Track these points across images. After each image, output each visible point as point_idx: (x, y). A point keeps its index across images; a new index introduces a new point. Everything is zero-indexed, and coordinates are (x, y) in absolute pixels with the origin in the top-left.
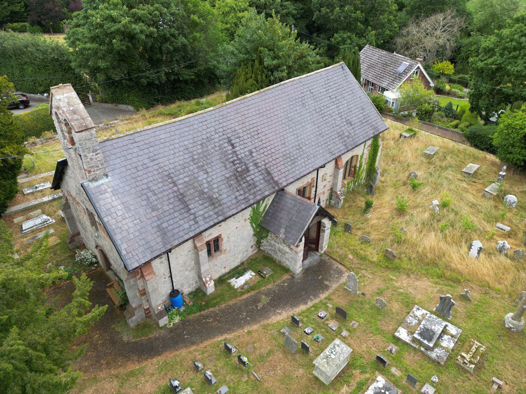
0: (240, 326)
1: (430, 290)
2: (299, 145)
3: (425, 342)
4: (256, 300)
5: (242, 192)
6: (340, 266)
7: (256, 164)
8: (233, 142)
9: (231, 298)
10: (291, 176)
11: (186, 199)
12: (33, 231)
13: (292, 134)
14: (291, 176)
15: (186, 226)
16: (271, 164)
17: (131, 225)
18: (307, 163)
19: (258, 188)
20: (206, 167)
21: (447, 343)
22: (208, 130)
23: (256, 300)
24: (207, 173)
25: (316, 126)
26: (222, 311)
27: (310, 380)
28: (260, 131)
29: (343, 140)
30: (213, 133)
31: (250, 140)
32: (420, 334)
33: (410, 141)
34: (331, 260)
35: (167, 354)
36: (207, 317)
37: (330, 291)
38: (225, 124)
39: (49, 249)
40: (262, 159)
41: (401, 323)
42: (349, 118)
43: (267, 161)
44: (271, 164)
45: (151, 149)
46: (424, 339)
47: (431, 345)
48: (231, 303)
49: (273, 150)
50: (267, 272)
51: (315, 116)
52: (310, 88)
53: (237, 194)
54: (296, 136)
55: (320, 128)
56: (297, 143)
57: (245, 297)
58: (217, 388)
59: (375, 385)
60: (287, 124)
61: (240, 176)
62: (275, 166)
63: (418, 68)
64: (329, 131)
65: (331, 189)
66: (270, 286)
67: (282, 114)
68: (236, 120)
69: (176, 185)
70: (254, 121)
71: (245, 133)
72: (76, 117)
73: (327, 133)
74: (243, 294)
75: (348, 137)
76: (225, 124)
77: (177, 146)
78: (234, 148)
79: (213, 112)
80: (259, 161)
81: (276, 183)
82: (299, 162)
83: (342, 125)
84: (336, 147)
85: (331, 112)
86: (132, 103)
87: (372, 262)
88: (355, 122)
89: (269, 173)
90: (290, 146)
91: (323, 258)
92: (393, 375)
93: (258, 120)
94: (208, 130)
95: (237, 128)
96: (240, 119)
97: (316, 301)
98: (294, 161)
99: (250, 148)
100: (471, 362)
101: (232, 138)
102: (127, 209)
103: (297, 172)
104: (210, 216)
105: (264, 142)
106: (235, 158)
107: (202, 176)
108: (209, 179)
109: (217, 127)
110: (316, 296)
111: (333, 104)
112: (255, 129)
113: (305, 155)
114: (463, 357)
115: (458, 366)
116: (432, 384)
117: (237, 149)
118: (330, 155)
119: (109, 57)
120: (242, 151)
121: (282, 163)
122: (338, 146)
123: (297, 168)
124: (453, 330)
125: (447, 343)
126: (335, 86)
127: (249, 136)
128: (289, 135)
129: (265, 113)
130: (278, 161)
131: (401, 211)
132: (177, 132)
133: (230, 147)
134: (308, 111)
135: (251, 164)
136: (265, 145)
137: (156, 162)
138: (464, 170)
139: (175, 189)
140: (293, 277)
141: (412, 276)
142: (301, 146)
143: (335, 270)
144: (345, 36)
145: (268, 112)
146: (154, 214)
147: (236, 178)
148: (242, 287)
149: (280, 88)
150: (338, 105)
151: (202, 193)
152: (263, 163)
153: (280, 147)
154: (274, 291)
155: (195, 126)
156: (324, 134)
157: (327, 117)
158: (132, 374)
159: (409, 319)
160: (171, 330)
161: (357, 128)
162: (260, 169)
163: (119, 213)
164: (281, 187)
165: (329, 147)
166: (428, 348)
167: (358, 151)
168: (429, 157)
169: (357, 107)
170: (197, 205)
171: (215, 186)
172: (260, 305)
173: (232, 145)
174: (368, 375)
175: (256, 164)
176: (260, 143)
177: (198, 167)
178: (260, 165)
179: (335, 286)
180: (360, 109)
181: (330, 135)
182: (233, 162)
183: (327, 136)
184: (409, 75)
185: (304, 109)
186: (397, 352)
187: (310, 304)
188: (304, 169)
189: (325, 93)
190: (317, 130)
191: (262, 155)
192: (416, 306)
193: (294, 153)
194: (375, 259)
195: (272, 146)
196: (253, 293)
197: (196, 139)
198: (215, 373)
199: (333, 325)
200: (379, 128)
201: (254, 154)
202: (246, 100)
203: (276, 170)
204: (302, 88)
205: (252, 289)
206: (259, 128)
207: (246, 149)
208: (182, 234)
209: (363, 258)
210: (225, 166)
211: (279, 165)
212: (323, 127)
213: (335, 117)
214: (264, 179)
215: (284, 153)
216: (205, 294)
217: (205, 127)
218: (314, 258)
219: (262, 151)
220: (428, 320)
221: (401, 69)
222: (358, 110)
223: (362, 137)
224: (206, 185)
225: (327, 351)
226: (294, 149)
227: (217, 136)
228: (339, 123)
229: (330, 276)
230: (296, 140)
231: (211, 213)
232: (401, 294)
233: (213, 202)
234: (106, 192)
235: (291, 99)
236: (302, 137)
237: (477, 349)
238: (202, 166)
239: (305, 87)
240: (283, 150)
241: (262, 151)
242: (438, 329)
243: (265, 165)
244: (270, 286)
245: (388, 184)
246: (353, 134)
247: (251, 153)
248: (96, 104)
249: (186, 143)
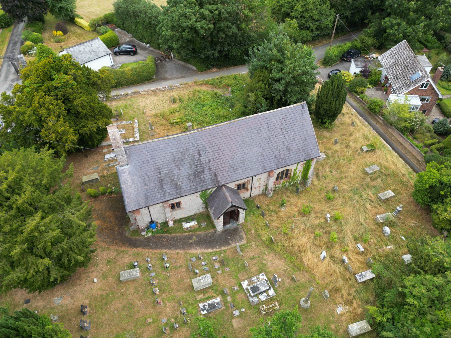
0: (176, 249)
1: (281, 267)
2: (243, 160)
3: (251, 292)
4: (190, 238)
5: (195, 184)
6: (244, 235)
8: (201, 153)
9: (179, 232)
10: (229, 179)
11: (163, 183)
12: (109, 160)
13: (242, 152)
14: (229, 179)
15: (159, 196)
16: (219, 170)
17: (133, 191)
18: (243, 173)
19: (205, 183)
20: (180, 166)
21: (263, 297)
22: (189, 144)
24: (179, 170)
25: (261, 149)
26: (172, 238)
27: (190, 286)
28: (220, 148)
29: (277, 161)
30: (191, 146)
31: (212, 153)
32: (252, 288)
33: (365, 154)
34: (242, 230)
35: (139, 249)
36: (164, 238)
37: (229, 247)
38: (199, 142)
39: (112, 174)
40: (215, 166)
41: (249, 279)
42: (290, 145)
43: (217, 168)
44: (219, 170)
45: (153, 153)
46: (251, 291)
47: (252, 295)
48: (178, 235)
49: (224, 162)
50: (203, 225)
51: (263, 141)
52: (268, 122)
53: (192, 184)
54: (244, 154)
55: (263, 151)
56: (242, 159)
57: (186, 234)
58: (151, 272)
59: (214, 300)
60: (241, 145)
61: (198, 174)
62: (222, 172)
63: (428, 81)
64: (269, 154)
65: (266, 185)
66: (201, 233)
67: (240, 139)
68: (208, 140)
69: (160, 174)
70: (220, 141)
71: (210, 149)
72: (115, 141)
73: (267, 154)
74: (186, 232)
75: (283, 159)
76: (199, 142)
77: (168, 152)
78: (200, 157)
79: (195, 134)
80: (212, 167)
81: (218, 182)
82: (238, 171)
83: (282, 150)
84: (269, 165)
85: (277, 140)
86: (195, 65)
87: (262, 240)
88: (294, 149)
89: (216, 175)
90: (237, 160)
91: (238, 227)
92: (227, 300)
93: (222, 141)
94: (189, 144)
95: (206, 145)
96: (210, 139)
97: (218, 250)
98: (235, 170)
99: (209, 158)
100: (265, 311)
101: (201, 151)
102: (133, 183)
103: (234, 178)
104: (173, 194)
105: (220, 155)
106: (199, 163)
107: (176, 171)
108: (179, 174)
109: (194, 143)
110: (220, 247)
111: (282, 134)
112: (218, 146)
113: (245, 168)
114: (263, 307)
115: (259, 309)
116: (240, 312)
117: (201, 158)
118: (263, 169)
119: (180, 42)
120: (204, 159)
121: (227, 170)
122: (272, 165)
123: (235, 175)
124: (271, 292)
125: (263, 297)
126: (289, 120)
127: (212, 150)
128: (238, 153)
129: (228, 137)
130: (225, 168)
131: (303, 214)
132: (170, 144)
133: (198, 156)
134: (260, 138)
135: (207, 168)
136: (220, 158)
137: (154, 160)
138: (379, 195)
139: (159, 176)
140: (216, 232)
141: (277, 256)
142: (244, 161)
143: (239, 236)
144: (394, 22)
145: (231, 136)
146: (145, 187)
147: (195, 176)
148: (187, 229)
149: (246, 120)
150: (285, 135)
151: (173, 180)
152: (215, 168)
153: (229, 160)
154: (201, 237)
155: (181, 142)
156: (264, 155)
157: (272, 143)
158: (123, 252)
160: (146, 239)
161: (292, 154)
162: (211, 172)
163: (129, 184)
164: (220, 184)
165: (265, 164)
166: (250, 295)
167: (293, 167)
168: (366, 174)
169: (301, 138)
170: (168, 186)
171: (181, 178)
172: (191, 241)
173: (200, 156)
174: (215, 295)
175: (210, 169)
176: (218, 156)
177: (175, 166)
178: (212, 169)
179: (233, 245)
180: (303, 139)
181: (269, 156)
182: (196, 165)
183: (266, 157)
184: (417, 85)
185: (258, 136)
186: (237, 291)
187: (215, 250)
188: (240, 176)
189: (279, 125)
190: (261, 151)
191: (216, 164)
192: (263, 273)
193: (238, 165)
194: (264, 239)
195: (224, 159)
196: (191, 233)
197: (179, 149)
198: (154, 266)
199: (217, 265)
200: (312, 155)
201: (211, 163)
202: (218, 127)
203: (221, 174)
204: (262, 121)
205: (191, 231)
206: (220, 146)
207: (207, 159)
208: (155, 200)
209: (259, 235)
210: (191, 167)
211: (224, 171)
212: (266, 150)
213: (279, 144)
214: (211, 178)
215: (231, 164)
216: (168, 225)
217: (187, 143)
218: (231, 226)
219: (217, 161)
220: (261, 283)
221: (415, 77)
222: (300, 140)
223: (293, 161)
224: (176, 177)
225: (201, 278)
226: (239, 162)
227: (193, 148)
228: (280, 148)
229: (235, 239)
230: (243, 156)
231: (174, 192)
232: (263, 263)
233: (177, 187)
234: (125, 172)
235: (250, 129)
236: (248, 155)
237: (273, 306)
238: (178, 165)
239: (264, 120)
240: (231, 162)
241: (217, 161)
242: (262, 289)
243: (215, 170)
244: (201, 233)
245: (316, 188)
246: (287, 158)
247: (210, 161)
248: (175, 59)
249: (173, 151)
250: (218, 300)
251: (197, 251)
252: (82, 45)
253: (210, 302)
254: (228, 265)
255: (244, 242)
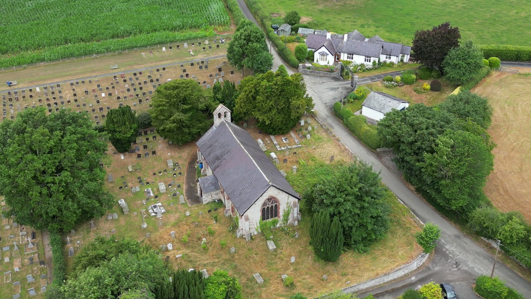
0: (186, 179)
7: (221, 162)
23: (193, 183)
32: (156, 206)
36: (195, 174)
89: (218, 167)
110: (186, 196)
151: (212, 150)
159: (163, 208)
175: (221, 162)
250: (152, 195)
251: (184, 187)
252: (385, 97)
253: (151, 192)
254: (173, 198)
255: (190, 206)
